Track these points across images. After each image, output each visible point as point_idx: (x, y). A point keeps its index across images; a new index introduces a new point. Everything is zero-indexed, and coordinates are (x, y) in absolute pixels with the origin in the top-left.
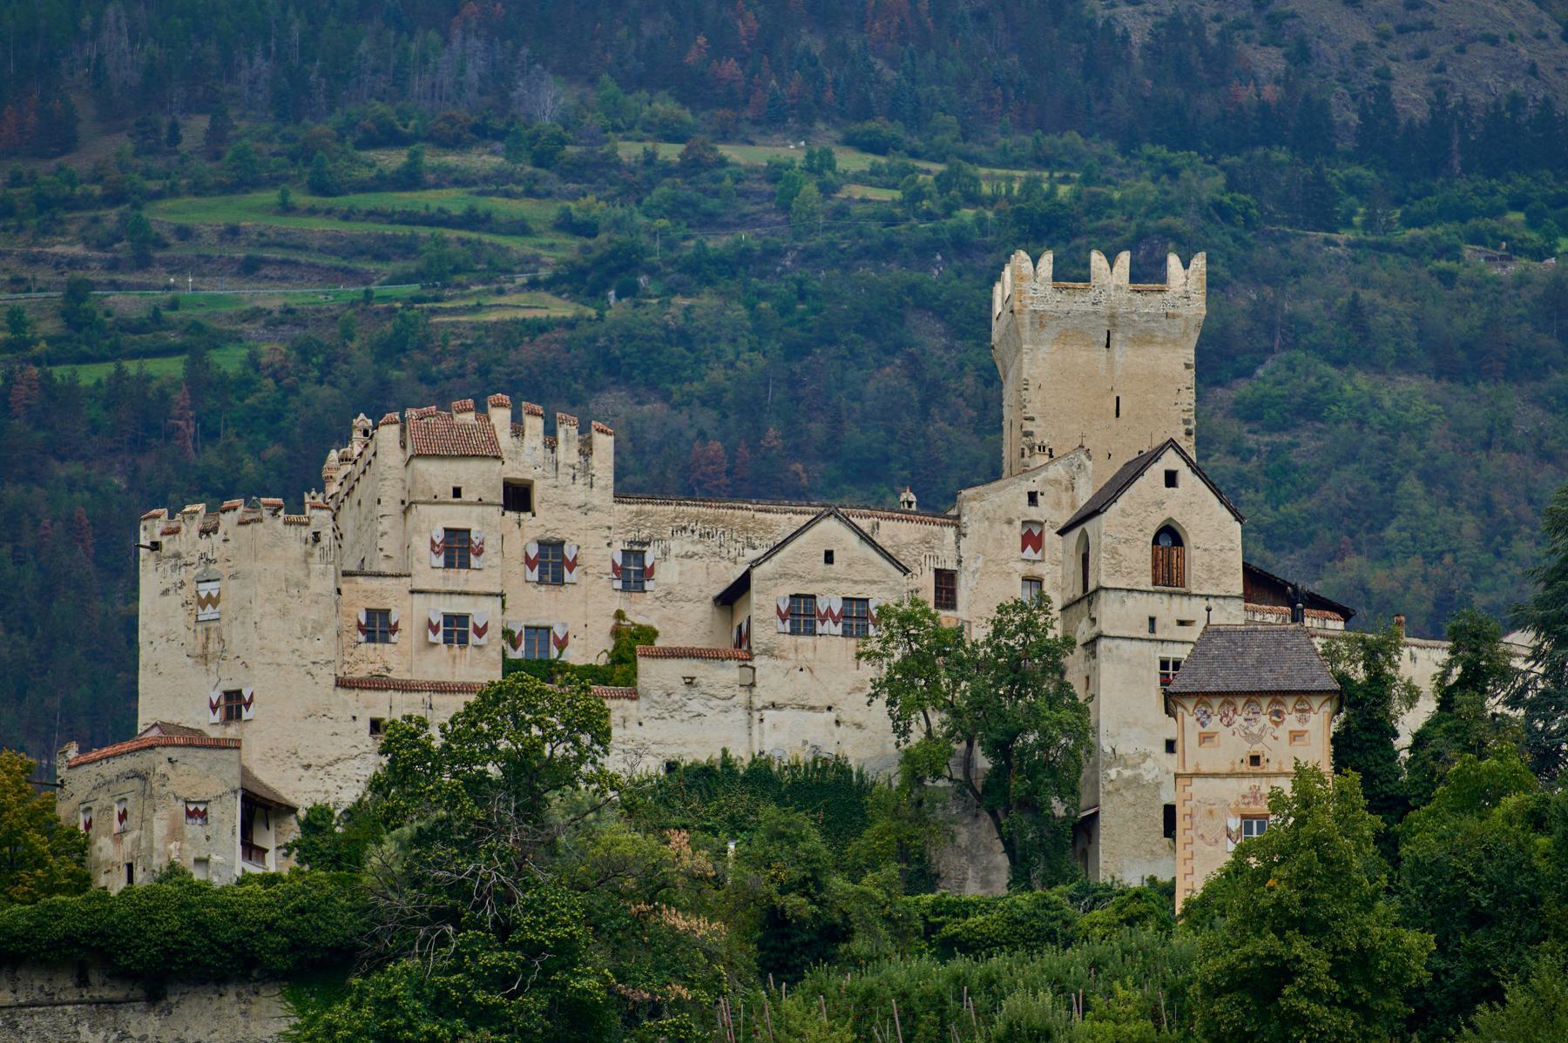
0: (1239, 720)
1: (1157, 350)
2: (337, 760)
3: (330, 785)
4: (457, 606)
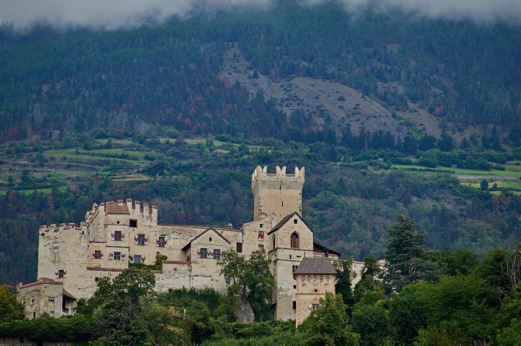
0: (312, 281)
1: (292, 190)
3: (85, 293)
4: (118, 250)
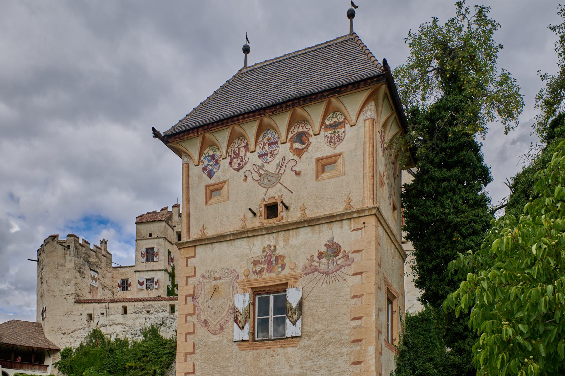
2: (75, 331)
3: (72, 340)
4: (150, 275)
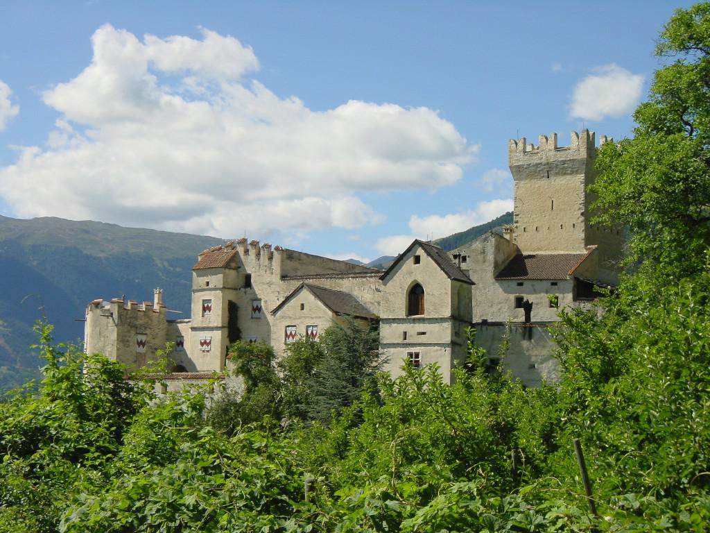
1: (568, 177)
